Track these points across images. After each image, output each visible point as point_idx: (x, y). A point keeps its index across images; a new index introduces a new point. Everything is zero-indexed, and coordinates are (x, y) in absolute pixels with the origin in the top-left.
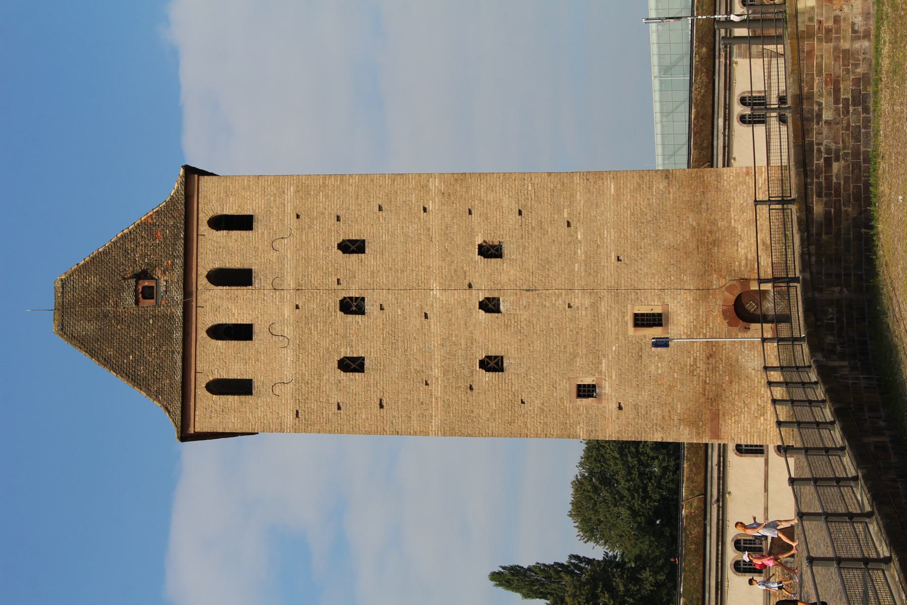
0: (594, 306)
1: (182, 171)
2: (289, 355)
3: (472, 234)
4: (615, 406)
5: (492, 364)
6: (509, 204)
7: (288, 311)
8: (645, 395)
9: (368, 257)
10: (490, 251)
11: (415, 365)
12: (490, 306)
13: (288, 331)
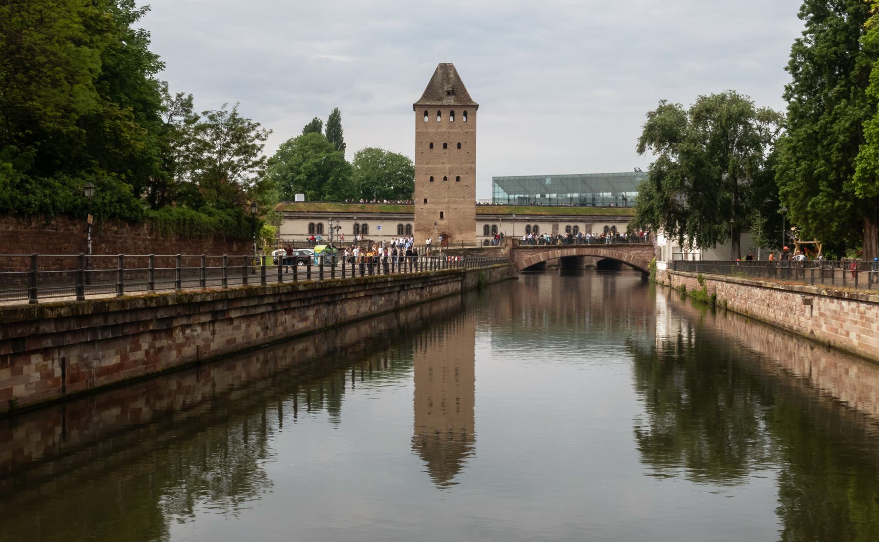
0: (445, 203)
2: (434, 130)
3: (462, 175)
5: (432, 179)
7: (444, 130)
8: (425, 214)
9: (456, 150)
10: (458, 179)
12: (445, 179)
13: (439, 130)
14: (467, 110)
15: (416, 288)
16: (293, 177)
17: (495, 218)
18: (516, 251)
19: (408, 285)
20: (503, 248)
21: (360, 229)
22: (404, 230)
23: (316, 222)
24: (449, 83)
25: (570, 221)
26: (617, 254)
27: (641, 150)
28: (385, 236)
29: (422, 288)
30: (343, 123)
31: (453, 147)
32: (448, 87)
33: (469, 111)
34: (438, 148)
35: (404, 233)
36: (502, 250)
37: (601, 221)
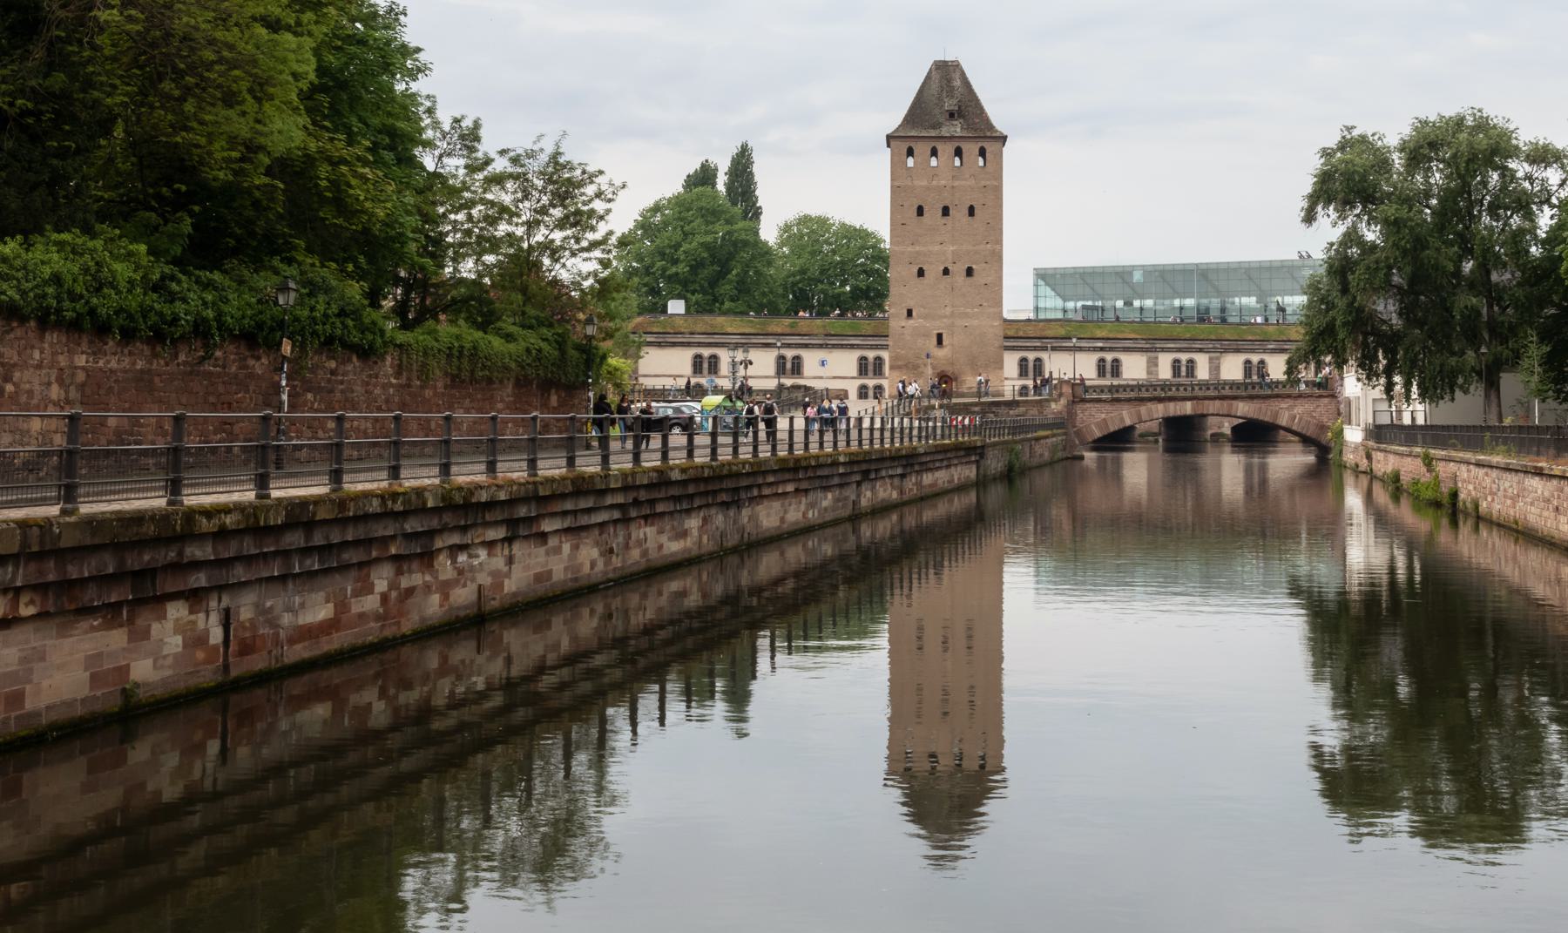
0: (945, 317)
2: (924, 183)
3: (976, 263)
5: (921, 273)
6: (989, 280)
7: (943, 182)
8: (909, 338)
9: (966, 219)
10: (970, 272)
12: (946, 272)
14: (986, 145)
15: (891, 477)
16: (664, 270)
17: (1038, 344)
18: (1079, 408)
19: (877, 471)
20: (1055, 401)
21: (789, 366)
22: (871, 368)
23: (706, 352)
24: (953, 97)
25: (1180, 350)
26: (1269, 413)
27: (1309, 218)
28: (835, 378)
29: (903, 476)
30: (757, 170)
31: (959, 214)
32: (949, 104)
34: (933, 215)
35: (870, 373)
36: (1053, 405)
37: (1238, 351)
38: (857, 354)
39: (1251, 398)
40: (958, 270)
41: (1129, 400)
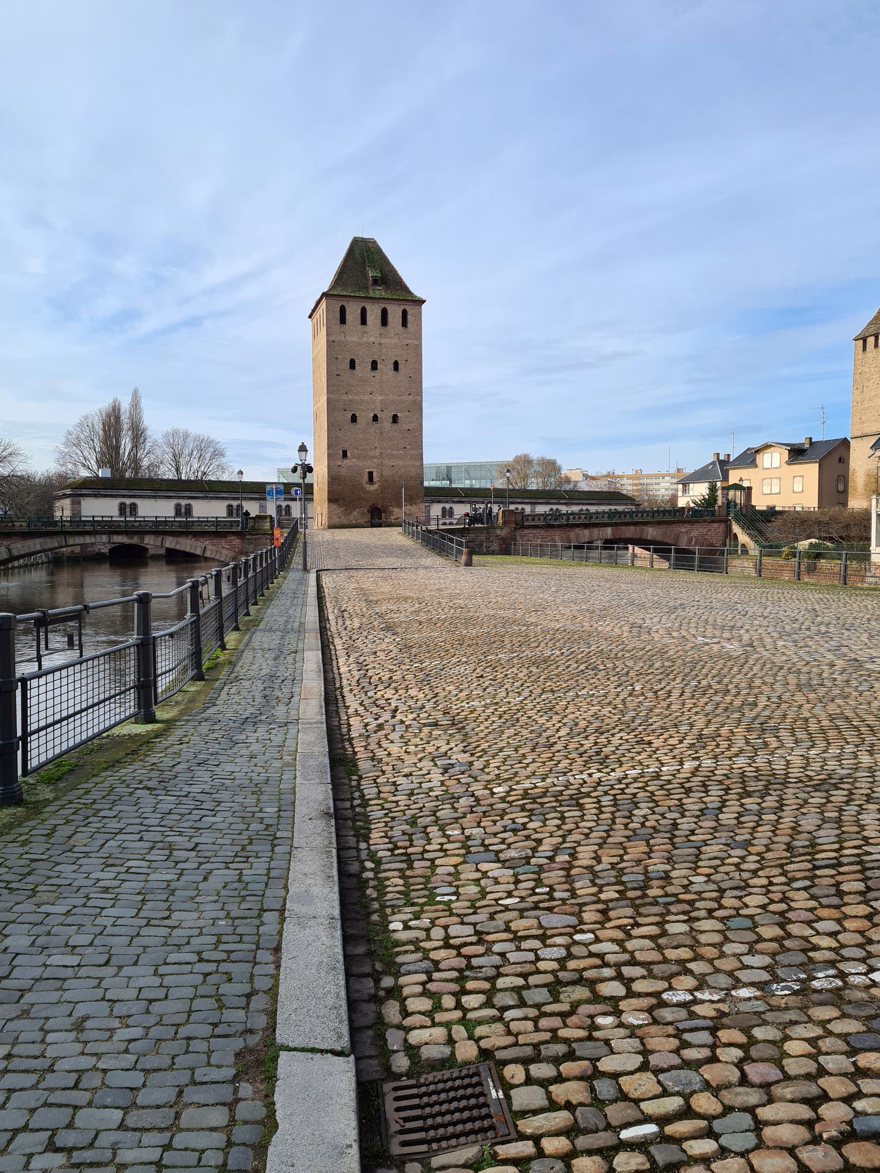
0: (375, 457)
1: (424, 298)
2: (355, 339)
3: (401, 412)
4: (340, 463)
5: (354, 419)
6: (412, 426)
7: (372, 339)
9: (392, 372)
10: (395, 419)
11: (353, 389)
12: (375, 418)
13: (364, 339)
21: (183, 510)
23: (128, 501)
31: (386, 368)
33: (411, 309)
34: (364, 367)
37: (439, 502)
38: (227, 503)
39: (659, 523)
40: (386, 417)
41: (559, 526)
